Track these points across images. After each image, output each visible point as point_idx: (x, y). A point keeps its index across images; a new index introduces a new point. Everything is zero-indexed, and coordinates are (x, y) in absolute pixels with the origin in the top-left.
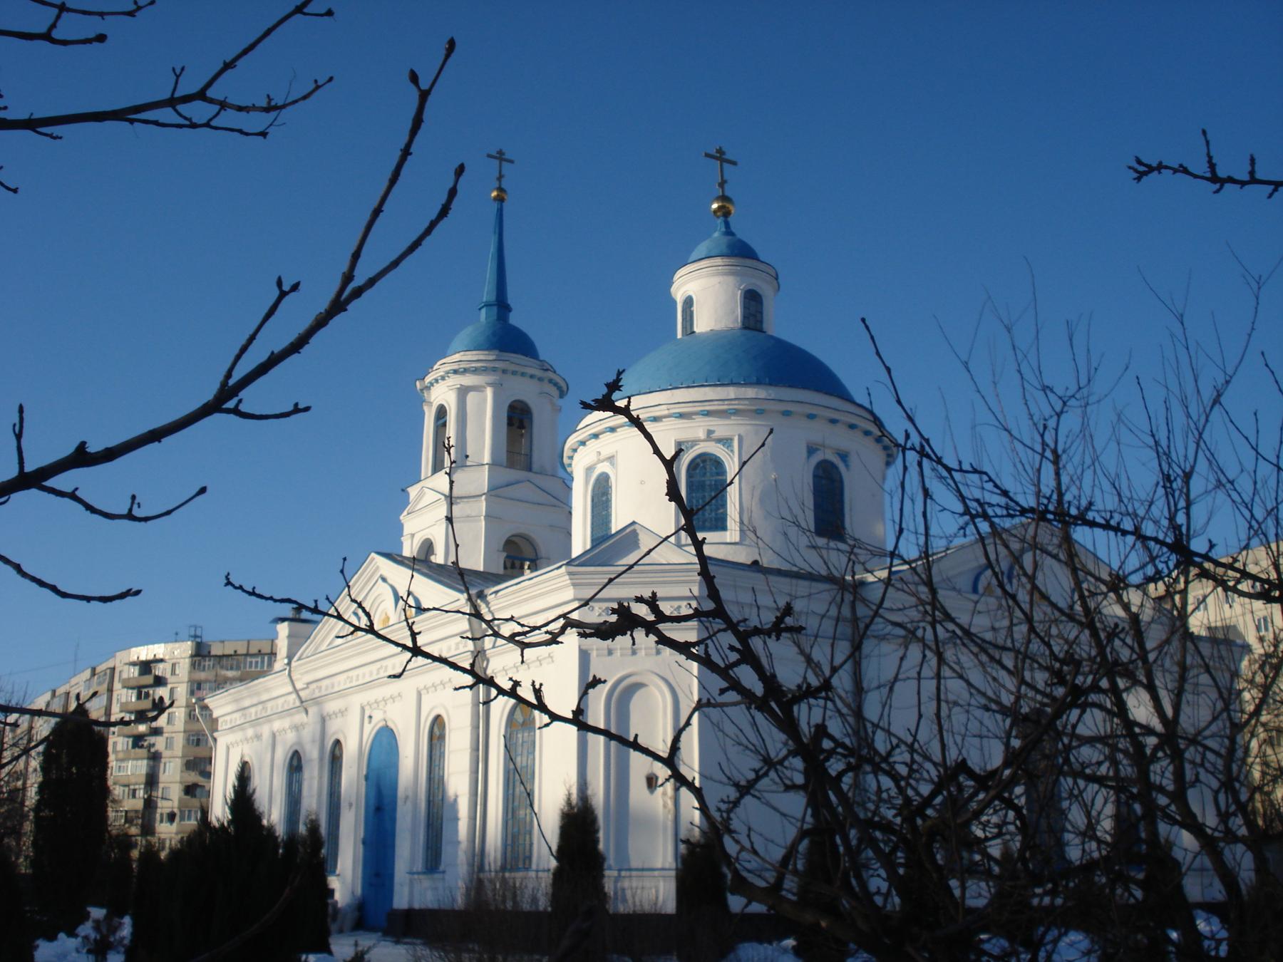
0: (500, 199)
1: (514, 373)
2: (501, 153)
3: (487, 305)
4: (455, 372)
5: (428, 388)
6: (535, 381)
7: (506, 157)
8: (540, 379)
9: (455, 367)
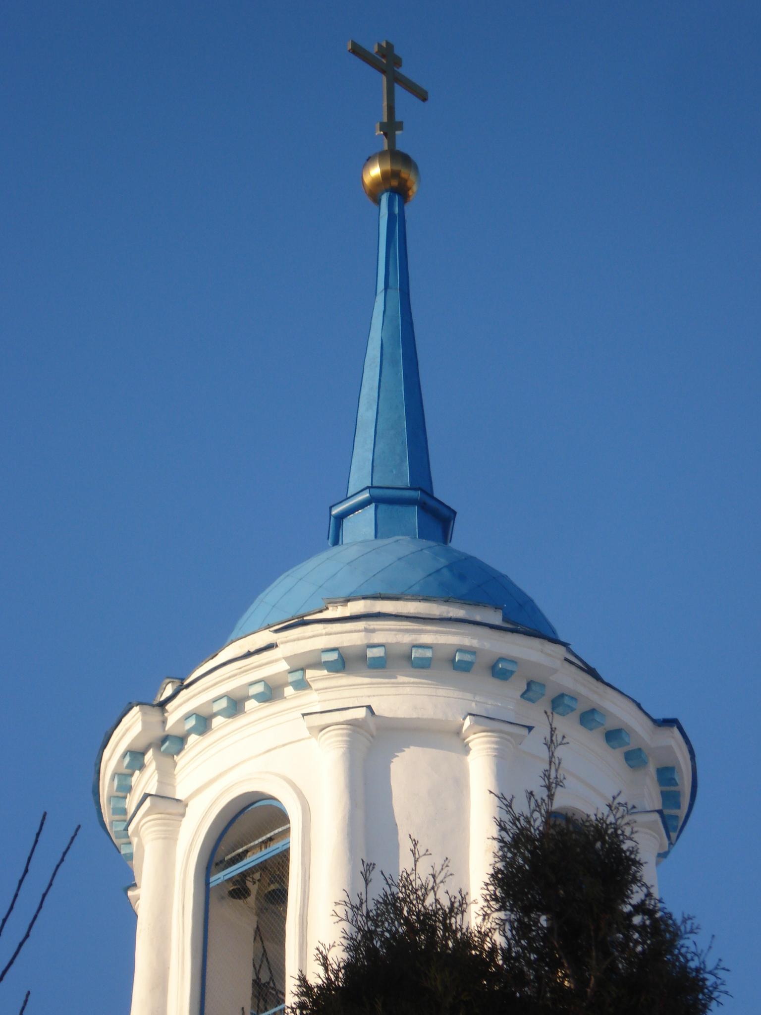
0: (396, 188)
1: (560, 703)
2: (387, 51)
3: (381, 499)
4: (343, 662)
5: (171, 744)
6: (614, 757)
7: (403, 71)
8: (635, 758)
9: (350, 637)
